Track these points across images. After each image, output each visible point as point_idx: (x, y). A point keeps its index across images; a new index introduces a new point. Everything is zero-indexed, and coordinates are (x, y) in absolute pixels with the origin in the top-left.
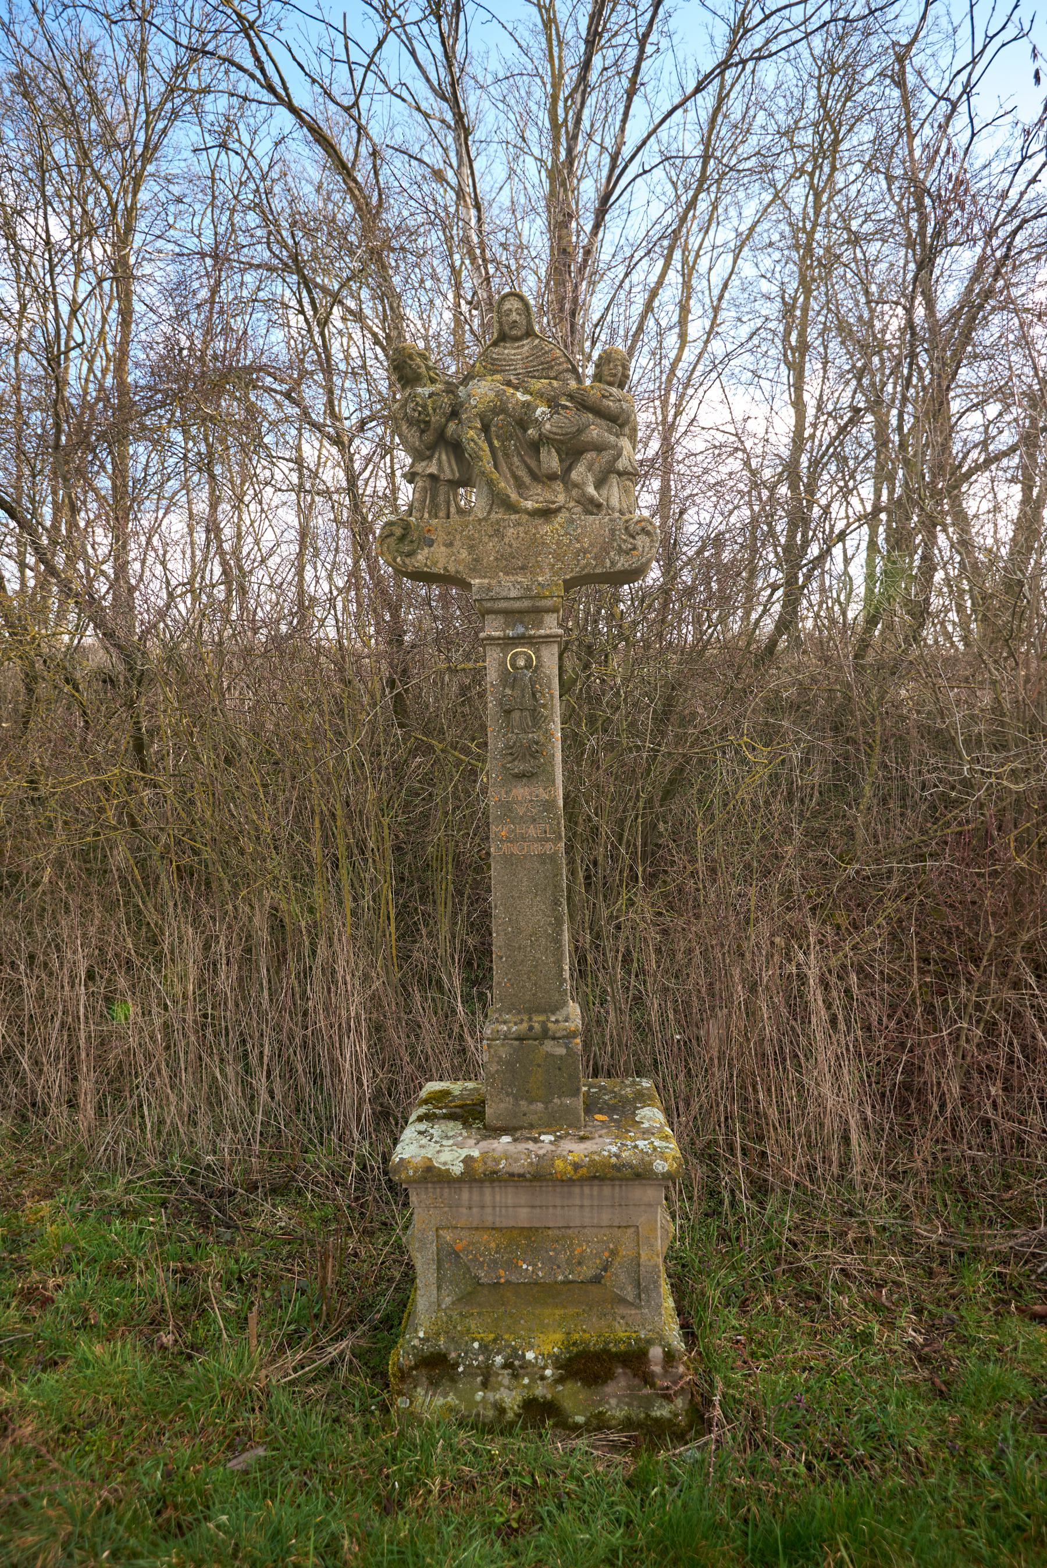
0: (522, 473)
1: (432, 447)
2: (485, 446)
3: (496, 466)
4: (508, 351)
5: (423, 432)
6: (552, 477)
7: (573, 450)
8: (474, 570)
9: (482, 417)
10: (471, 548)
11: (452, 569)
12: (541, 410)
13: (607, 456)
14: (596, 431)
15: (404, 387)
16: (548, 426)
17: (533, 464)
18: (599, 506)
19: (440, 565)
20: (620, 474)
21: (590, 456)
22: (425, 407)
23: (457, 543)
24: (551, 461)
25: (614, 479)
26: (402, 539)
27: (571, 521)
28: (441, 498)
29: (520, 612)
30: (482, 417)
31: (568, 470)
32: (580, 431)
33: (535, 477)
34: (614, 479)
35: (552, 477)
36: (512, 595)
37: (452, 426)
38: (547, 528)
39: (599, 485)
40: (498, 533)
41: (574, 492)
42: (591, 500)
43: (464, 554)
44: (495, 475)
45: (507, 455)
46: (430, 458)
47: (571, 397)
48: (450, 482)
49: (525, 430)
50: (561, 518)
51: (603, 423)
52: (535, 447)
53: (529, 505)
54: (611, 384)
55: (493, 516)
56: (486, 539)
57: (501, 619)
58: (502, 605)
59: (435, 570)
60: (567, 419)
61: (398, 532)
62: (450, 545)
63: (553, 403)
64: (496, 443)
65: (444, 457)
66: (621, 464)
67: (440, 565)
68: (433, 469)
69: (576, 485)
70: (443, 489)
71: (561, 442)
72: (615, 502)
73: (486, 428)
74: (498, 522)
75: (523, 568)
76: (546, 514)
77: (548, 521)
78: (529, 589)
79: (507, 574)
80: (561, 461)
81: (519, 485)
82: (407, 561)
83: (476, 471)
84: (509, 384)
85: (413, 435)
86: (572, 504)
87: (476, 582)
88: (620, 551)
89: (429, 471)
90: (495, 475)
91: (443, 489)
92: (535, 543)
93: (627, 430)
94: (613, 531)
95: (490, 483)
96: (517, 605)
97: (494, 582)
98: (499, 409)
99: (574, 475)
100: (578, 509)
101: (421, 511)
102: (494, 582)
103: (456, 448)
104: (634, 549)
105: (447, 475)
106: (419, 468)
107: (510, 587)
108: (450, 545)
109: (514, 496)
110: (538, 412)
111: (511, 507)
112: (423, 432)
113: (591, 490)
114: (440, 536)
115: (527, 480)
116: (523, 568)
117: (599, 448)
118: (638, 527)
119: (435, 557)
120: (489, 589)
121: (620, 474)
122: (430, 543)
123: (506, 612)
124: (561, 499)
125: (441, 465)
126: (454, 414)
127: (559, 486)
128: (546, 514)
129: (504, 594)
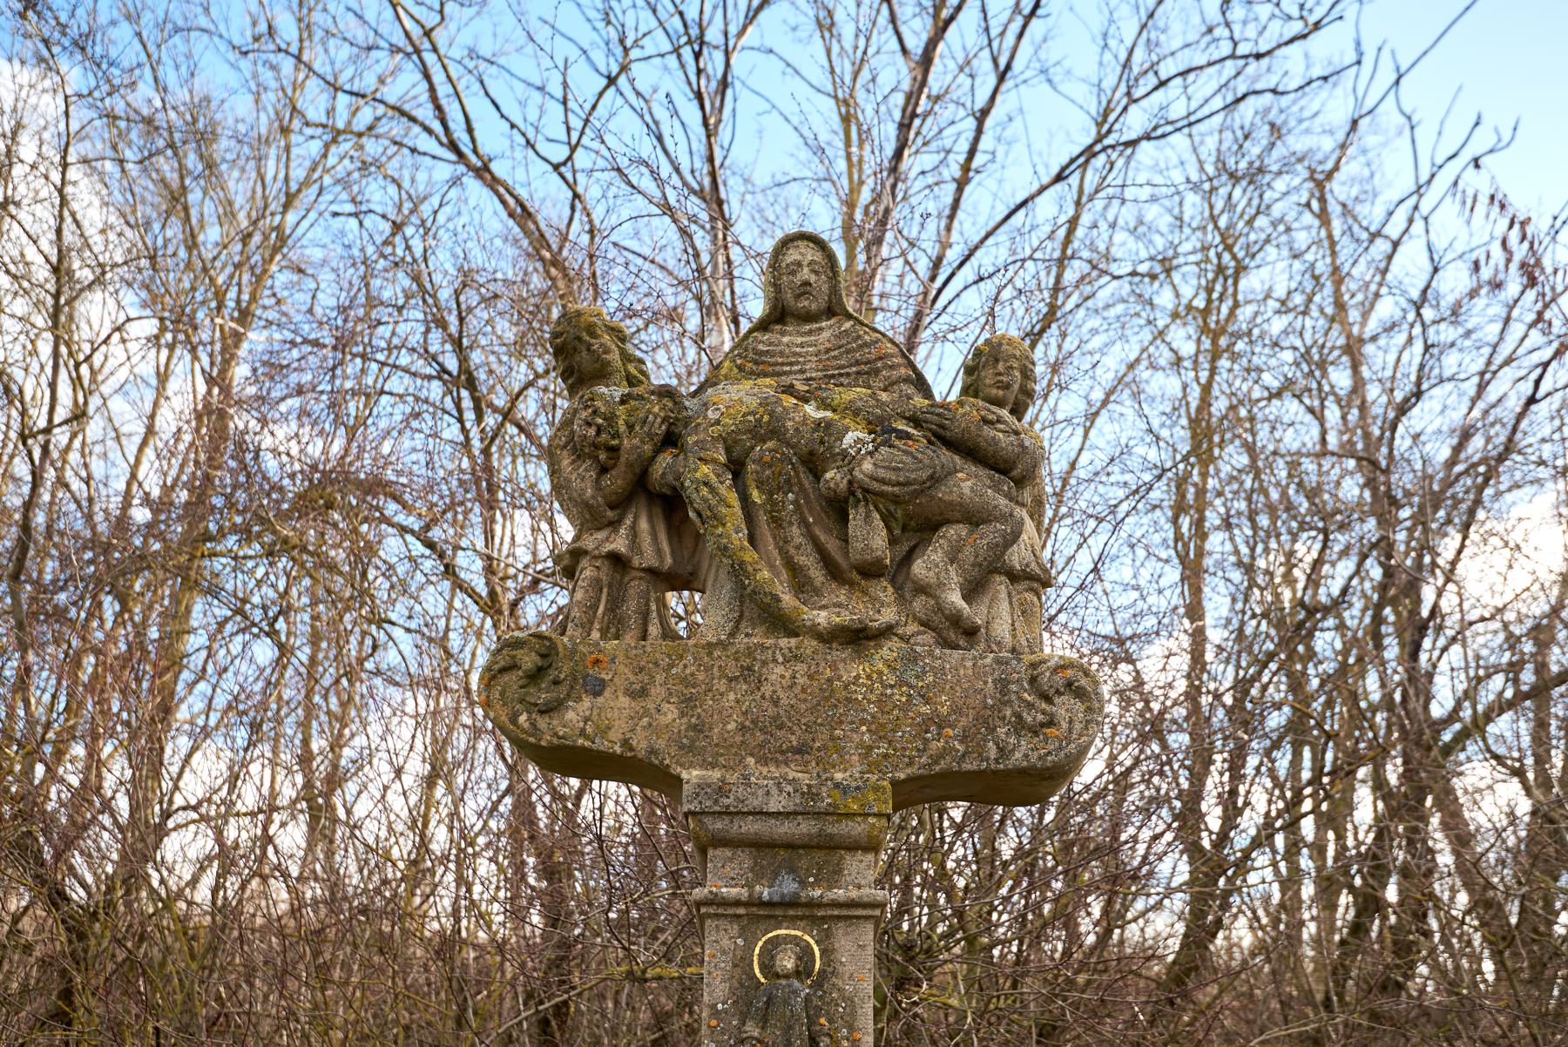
0: (807, 558)
1: (621, 503)
2: (733, 498)
3: (752, 539)
4: (790, 338)
5: (604, 470)
6: (871, 571)
7: (918, 521)
8: (690, 749)
9: (729, 444)
10: (688, 703)
11: (641, 744)
12: (853, 436)
13: (990, 534)
14: (968, 483)
15: (572, 390)
16: (867, 466)
17: (832, 545)
18: (971, 632)
19: (615, 735)
20: (1013, 577)
21: (953, 531)
22: (611, 418)
23: (657, 691)
24: (871, 536)
25: (1001, 585)
26: (536, 675)
27: (913, 658)
28: (631, 606)
29: (790, 846)
30: (729, 444)
31: (908, 559)
32: (935, 480)
33: (834, 572)
34: (1001, 585)
35: (871, 571)
36: (773, 806)
37: (665, 460)
38: (857, 669)
39: (973, 591)
40: (749, 674)
41: (919, 604)
42: (956, 620)
43: (671, 713)
44: (750, 556)
45: (776, 522)
46: (614, 525)
47: (916, 421)
48: (651, 572)
49: (817, 476)
50: (889, 650)
51: (983, 472)
52: (838, 508)
53: (822, 618)
54: (999, 403)
55: (741, 641)
56: (721, 685)
57: (745, 859)
58: (750, 827)
59: (601, 745)
60: (912, 457)
61: (529, 660)
62: (641, 693)
63: (880, 427)
64: (756, 496)
65: (644, 525)
66: (1017, 556)
67: (615, 735)
68: (619, 544)
69: (922, 589)
70: (636, 587)
71: (896, 500)
72: (1002, 629)
73: (736, 468)
74: (750, 651)
75: (800, 750)
76: (858, 638)
77: (860, 655)
78: (811, 794)
79: (763, 761)
80: (893, 541)
81: (801, 584)
82: (542, 722)
83: (710, 546)
84: (789, 390)
85: (583, 479)
86: (912, 628)
87: (692, 776)
88: (1019, 726)
89: (609, 547)
90: (750, 556)
91: (636, 587)
92: (830, 697)
93: (1027, 496)
94: (1003, 685)
95: (739, 571)
96: (784, 829)
97: (733, 778)
98: (768, 428)
99: (919, 568)
100: (928, 637)
101: (587, 627)
102: (733, 778)
103: (672, 505)
104: (1051, 723)
105: (648, 558)
106: (589, 543)
107: (771, 788)
108: (641, 693)
109: (788, 599)
110: (849, 438)
111: (780, 623)
112: (604, 470)
113: (955, 598)
114: (623, 674)
115: (817, 574)
116: (800, 750)
117: (975, 518)
118: (1059, 679)
119: (609, 717)
120: (722, 789)
121: (1013, 577)
122: (598, 689)
123: (758, 845)
124: (888, 615)
125: (642, 537)
126: (671, 440)
127: (883, 590)
128: (858, 638)
129: (755, 803)
